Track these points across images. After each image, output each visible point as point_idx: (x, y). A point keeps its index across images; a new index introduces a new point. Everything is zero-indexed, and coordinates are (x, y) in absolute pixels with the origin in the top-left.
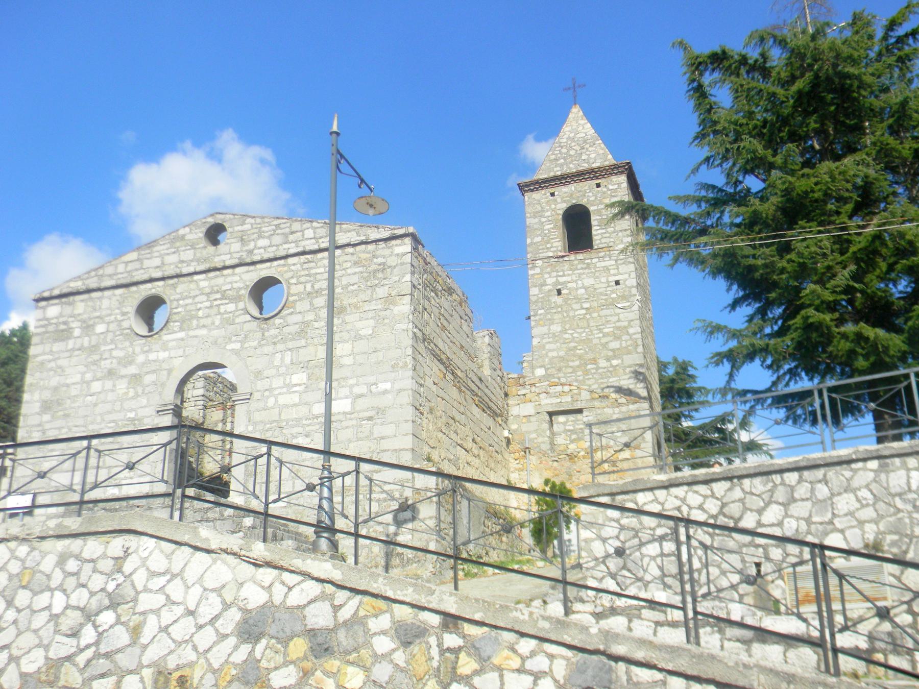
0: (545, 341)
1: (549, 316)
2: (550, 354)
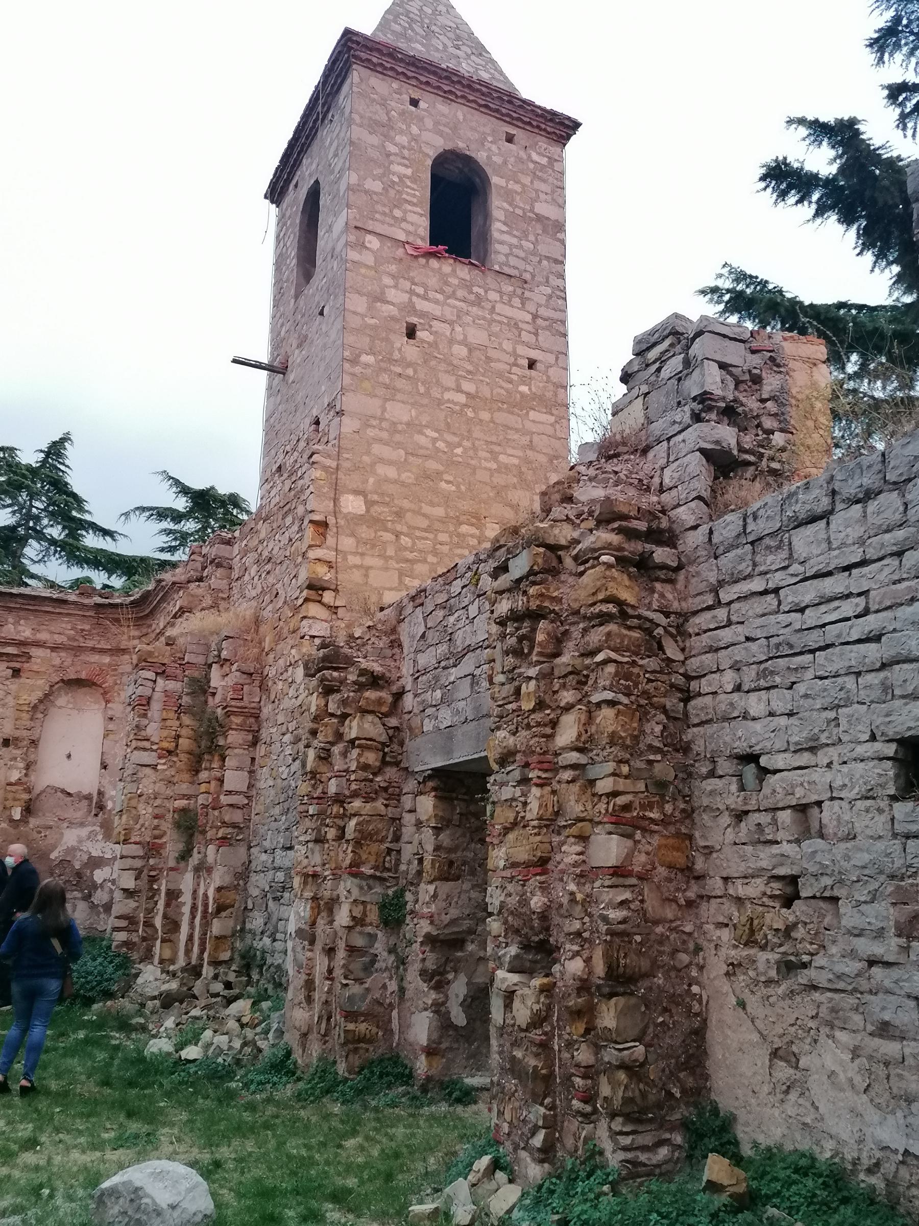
0: (371, 432)
1: (385, 378)
2: (381, 470)
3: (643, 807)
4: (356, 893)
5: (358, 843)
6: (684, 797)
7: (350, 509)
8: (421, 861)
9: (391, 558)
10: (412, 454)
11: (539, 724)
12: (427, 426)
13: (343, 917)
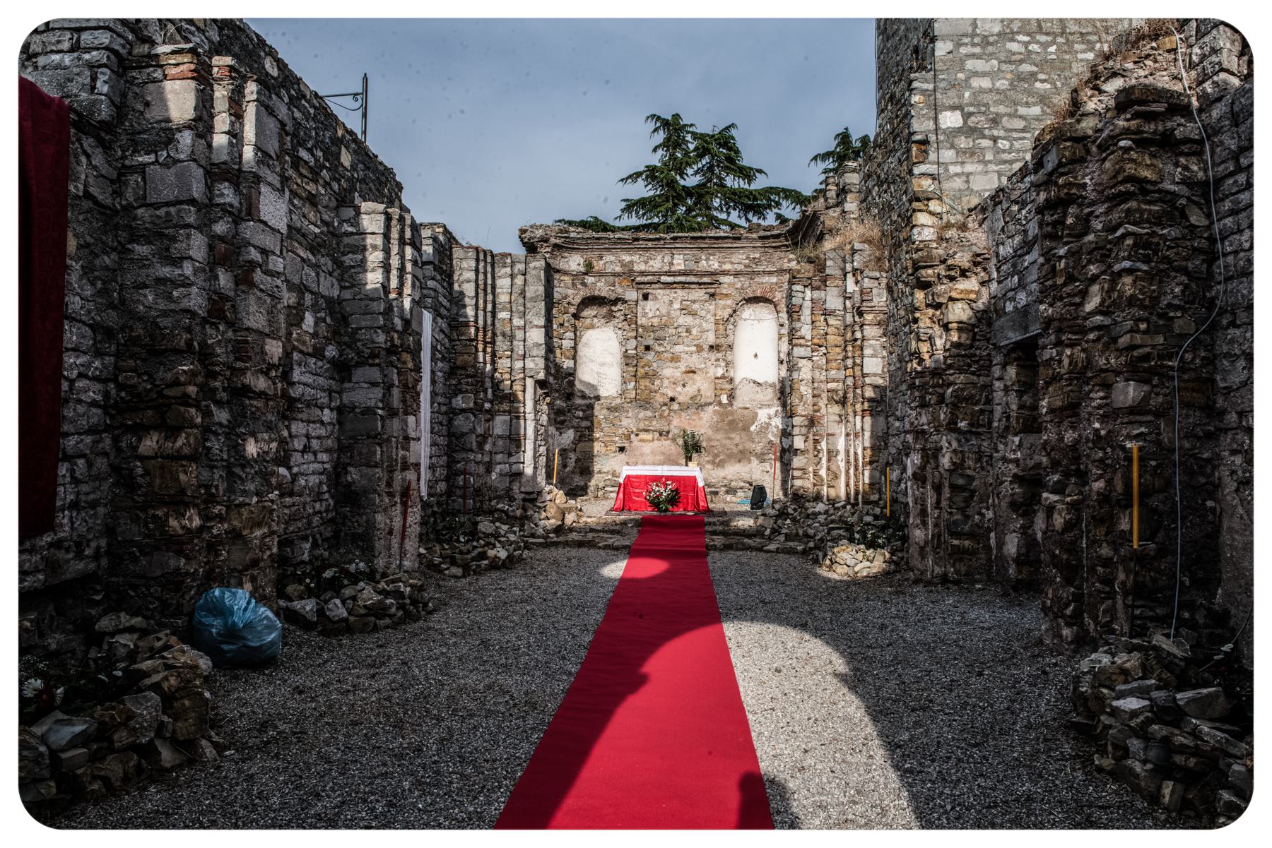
3: (1161, 357)
4: (955, 444)
5: (955, 406)
6: (1206, 346)
7: (949, 125)
8: (1008, 418)
9: (990, 162)
10: (1005, 62)
11: (1069, 295)
12: (1018, 33)
13: (945, 461)
